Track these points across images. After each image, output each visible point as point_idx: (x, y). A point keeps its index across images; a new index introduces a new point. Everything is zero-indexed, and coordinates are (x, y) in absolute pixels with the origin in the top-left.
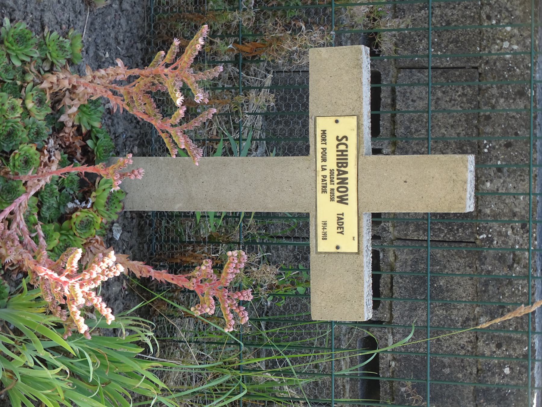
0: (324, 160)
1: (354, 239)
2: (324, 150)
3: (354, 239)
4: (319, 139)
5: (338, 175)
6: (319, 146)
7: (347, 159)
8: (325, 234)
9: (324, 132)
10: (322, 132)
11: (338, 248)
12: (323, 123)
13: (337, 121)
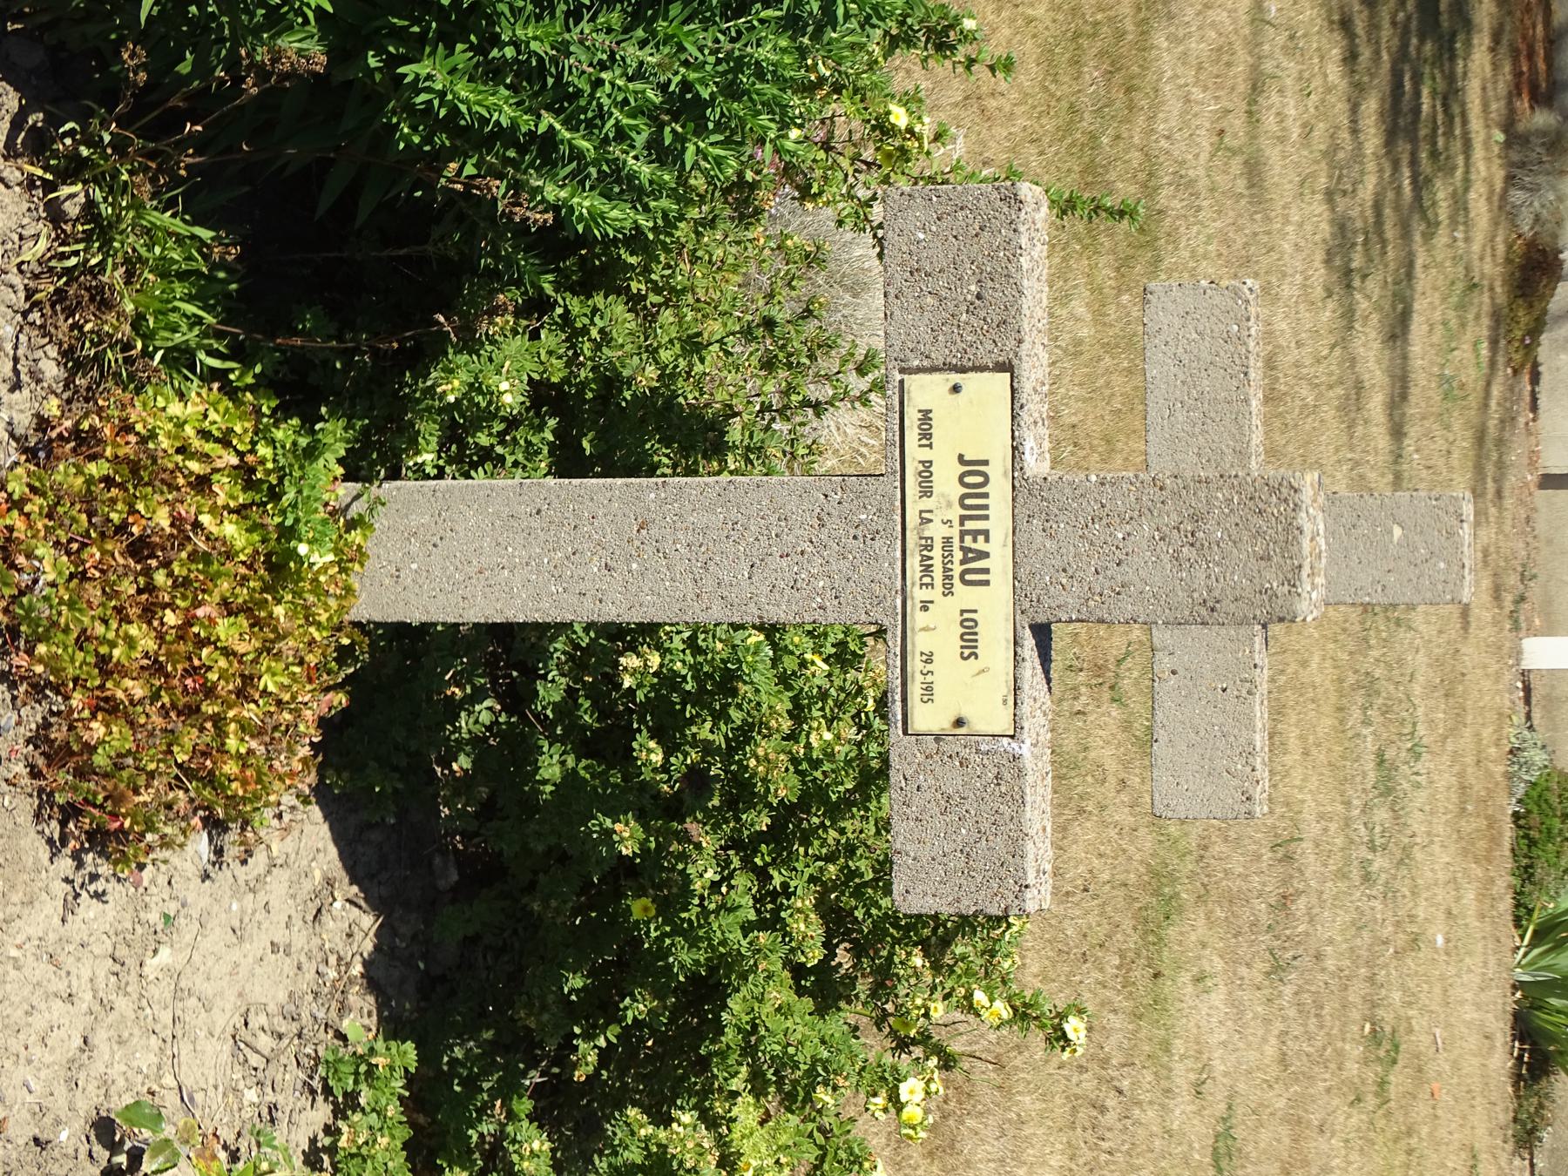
1: (1005, 702)
3: (1005, 702)
4: (912, 436)
5: (962, 562)
7: (986, 507)
8: (928, 689)
9: (926, 415)
10: (920, 415)
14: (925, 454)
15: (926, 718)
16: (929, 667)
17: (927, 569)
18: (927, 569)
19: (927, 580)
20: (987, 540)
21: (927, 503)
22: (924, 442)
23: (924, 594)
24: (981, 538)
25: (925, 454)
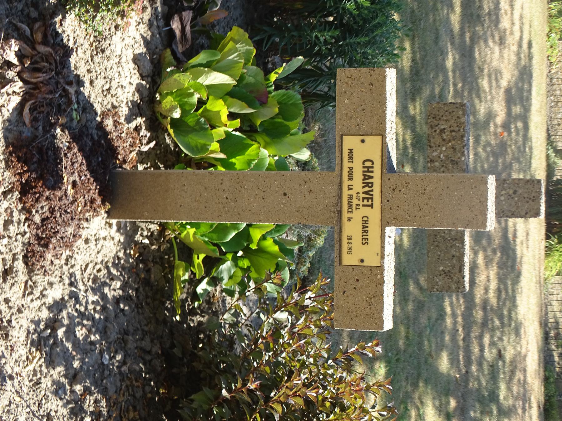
0: (350, 178)
1: (378, 254)
6: (346, 164)
8: (350, 249)
9: (351, 151)
11: (362, 261)
12: (350, 142)
13: (363, 141)
14: (350, 165)
15: (349, 260)
16: (350, 241)
17: (350, 206)
18: (350, 206)
19: (350, 210)
21: (350, 183)
22: (350, 160)
23: (350, 215)
25: (350, 165)
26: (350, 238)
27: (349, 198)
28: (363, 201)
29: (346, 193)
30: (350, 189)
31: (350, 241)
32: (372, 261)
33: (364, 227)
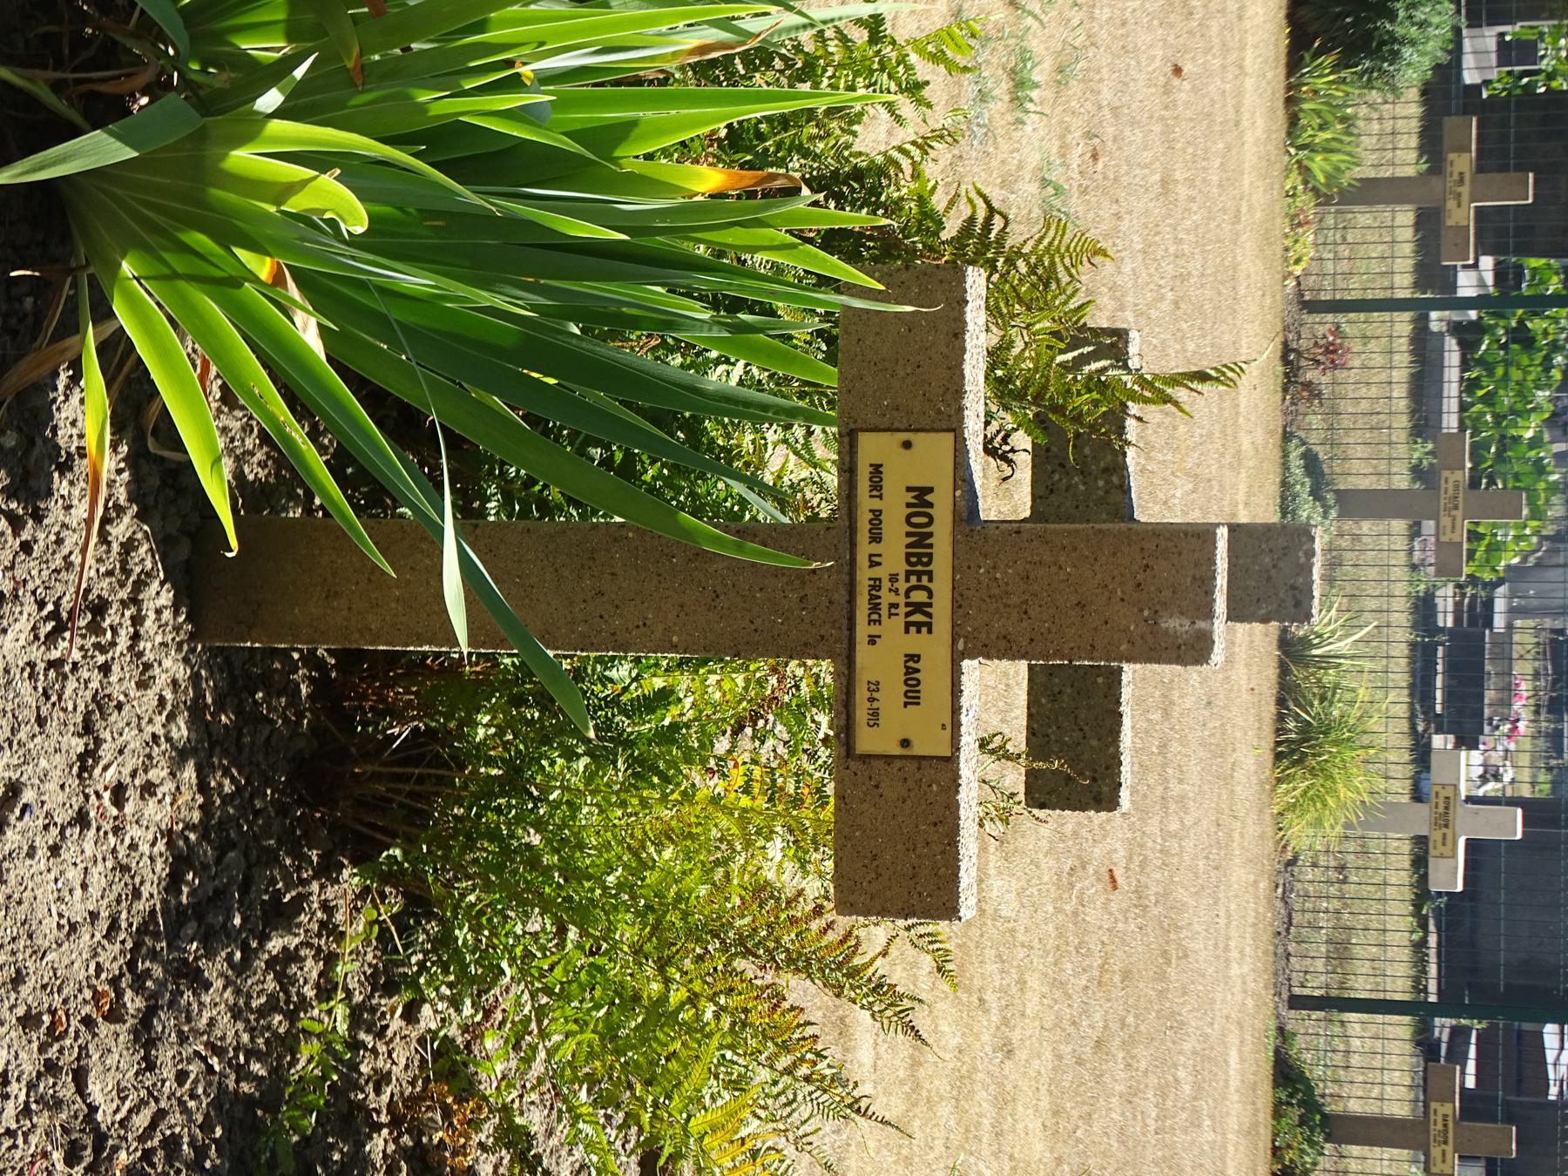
2: (877, 513)
6: (866, 503)
8: (875, 714)
9: (877, 469)
11: (905, 743)
13: (907, 445)
14: (876, 504)
16: (875, 695)
17: (875, 608)
18: (875, 608)
19: (874, 617)
20: (930, 580)
23: (874, 630)
24: (925, 579)
25: (876, 504)
26: (874, 687)
27: (873, 587)
28: (907, 580)
29: (864, 574)
30: (873, 564)
31: (875, 695)
32: (930, 744)
33: (910, 671)
